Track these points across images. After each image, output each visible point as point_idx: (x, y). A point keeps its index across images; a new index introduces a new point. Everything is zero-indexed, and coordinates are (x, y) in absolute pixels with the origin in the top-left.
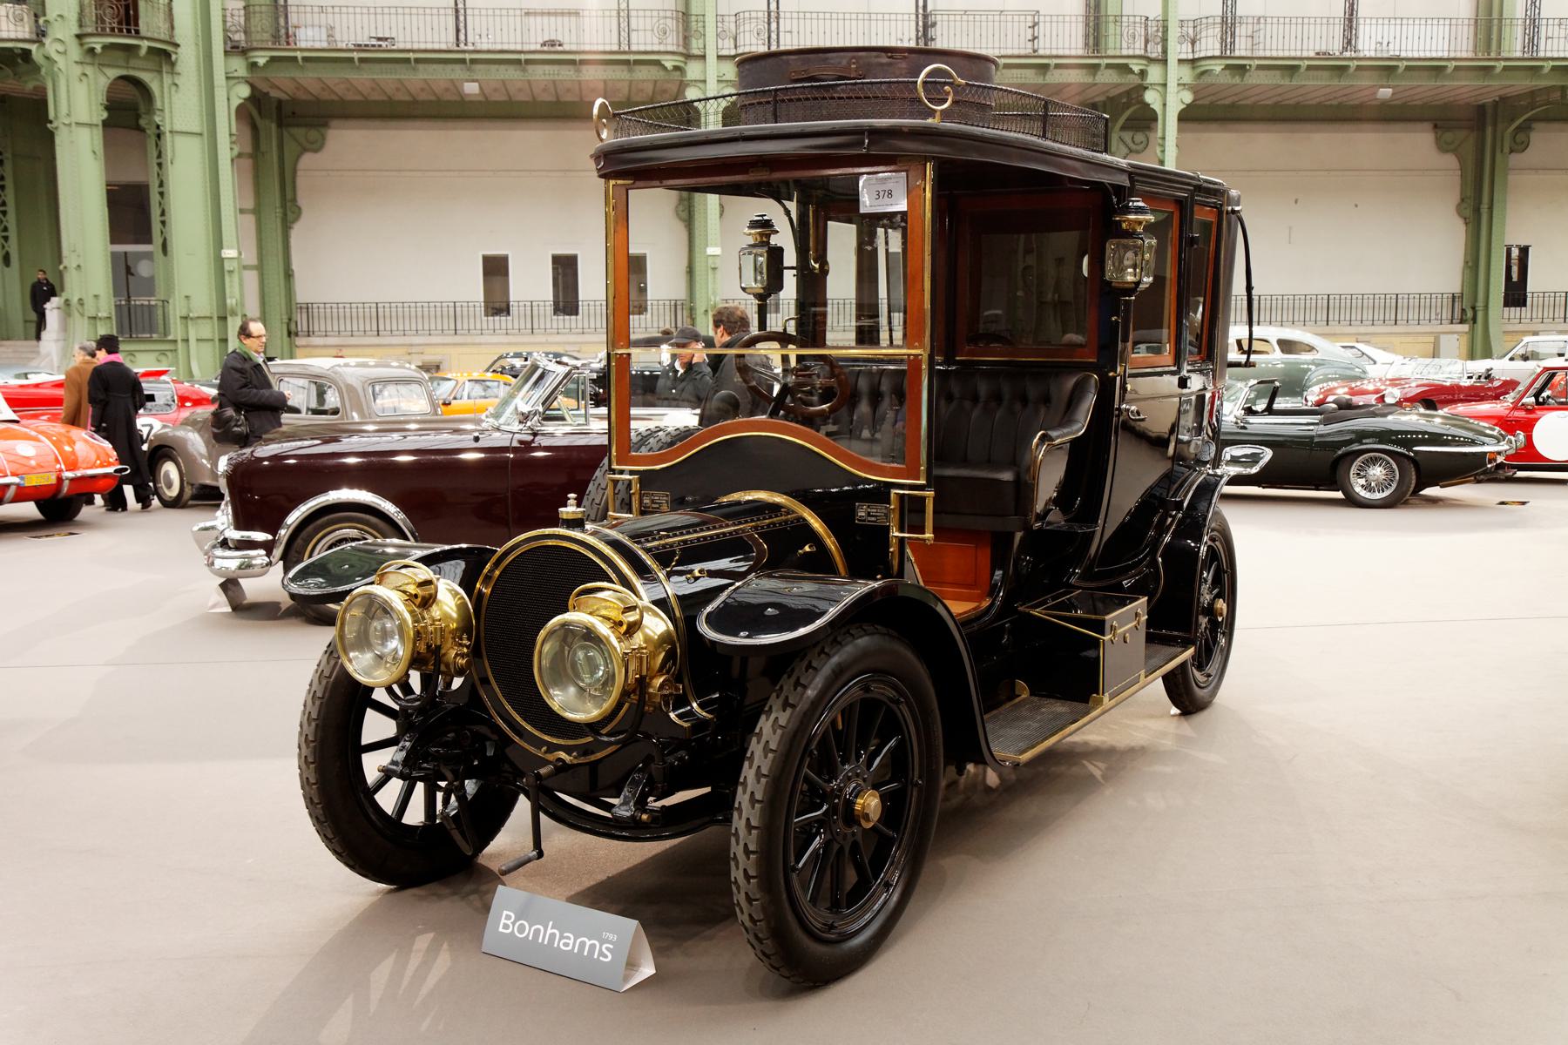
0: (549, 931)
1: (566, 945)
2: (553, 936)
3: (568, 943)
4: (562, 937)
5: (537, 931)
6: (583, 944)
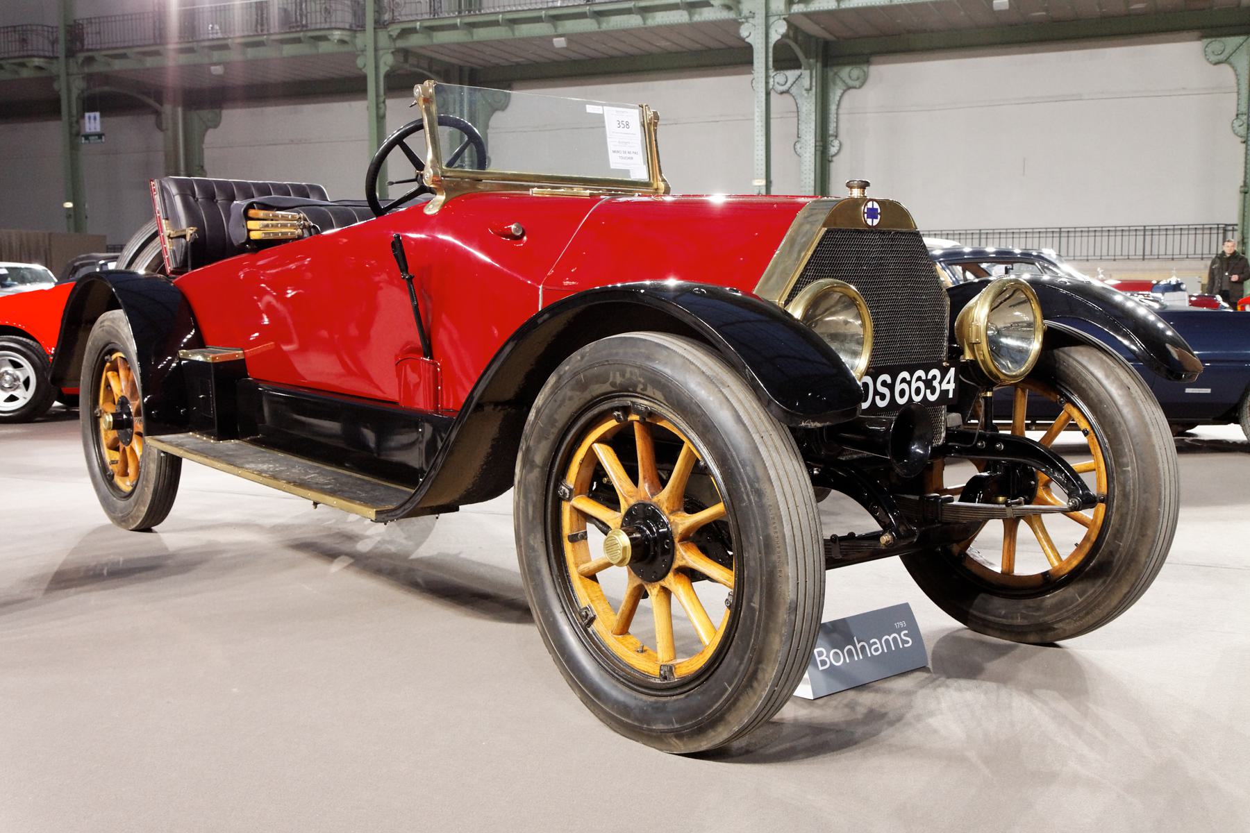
0: (858, 646)
1: (876, 650)
5: (849, 651)
6: (887, 641)
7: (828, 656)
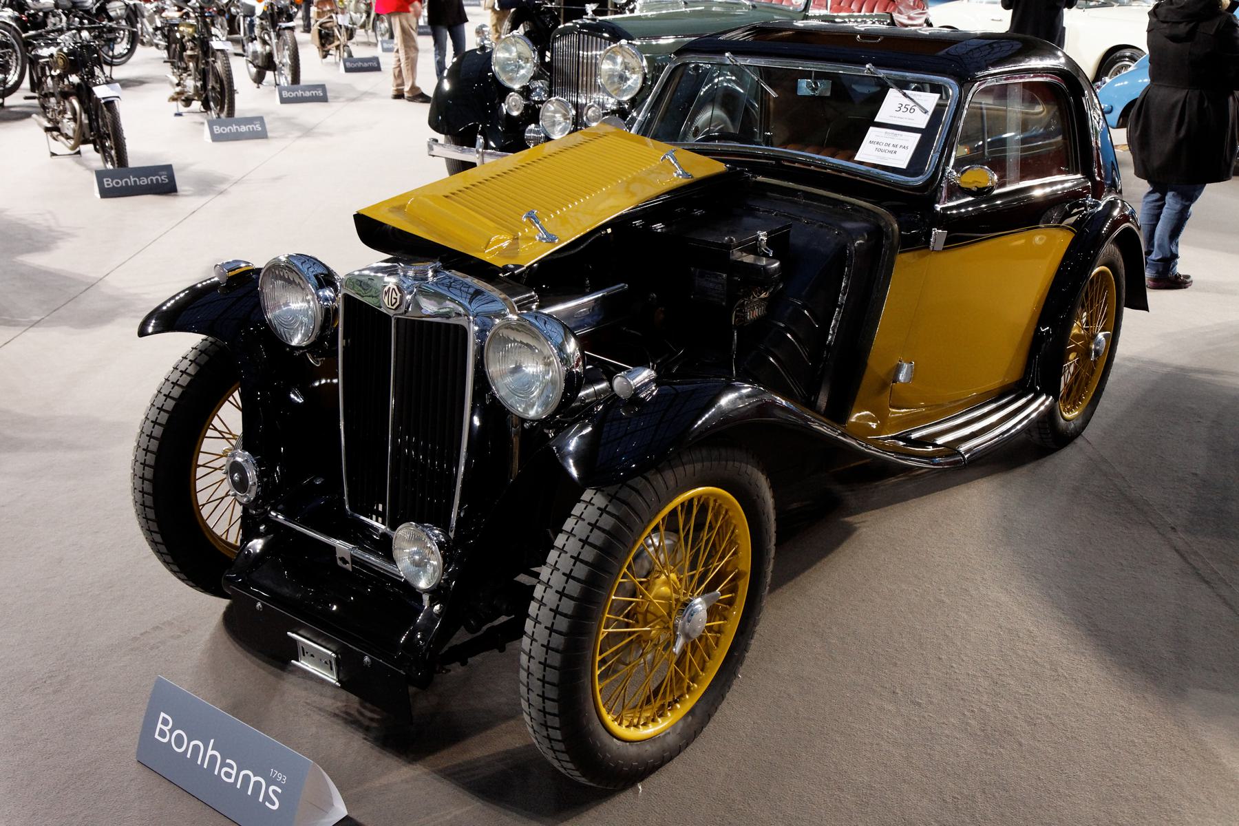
0: (210, 752)
1: (228, 775)
2: (213, 758)
3: (230, 773)
4: (223, 765)
5: (196, 748)
6: (246, 778)
7: (171, 731)
